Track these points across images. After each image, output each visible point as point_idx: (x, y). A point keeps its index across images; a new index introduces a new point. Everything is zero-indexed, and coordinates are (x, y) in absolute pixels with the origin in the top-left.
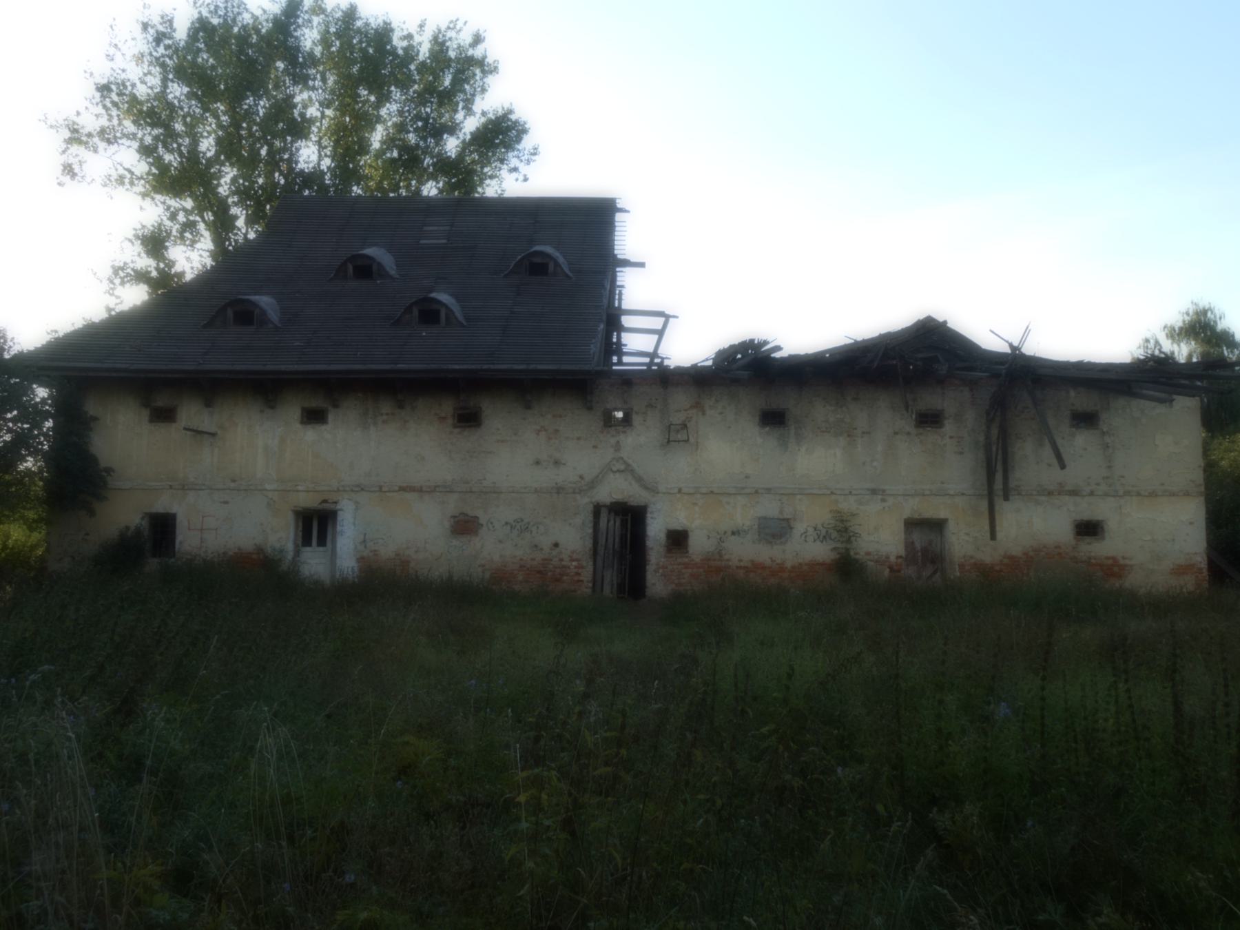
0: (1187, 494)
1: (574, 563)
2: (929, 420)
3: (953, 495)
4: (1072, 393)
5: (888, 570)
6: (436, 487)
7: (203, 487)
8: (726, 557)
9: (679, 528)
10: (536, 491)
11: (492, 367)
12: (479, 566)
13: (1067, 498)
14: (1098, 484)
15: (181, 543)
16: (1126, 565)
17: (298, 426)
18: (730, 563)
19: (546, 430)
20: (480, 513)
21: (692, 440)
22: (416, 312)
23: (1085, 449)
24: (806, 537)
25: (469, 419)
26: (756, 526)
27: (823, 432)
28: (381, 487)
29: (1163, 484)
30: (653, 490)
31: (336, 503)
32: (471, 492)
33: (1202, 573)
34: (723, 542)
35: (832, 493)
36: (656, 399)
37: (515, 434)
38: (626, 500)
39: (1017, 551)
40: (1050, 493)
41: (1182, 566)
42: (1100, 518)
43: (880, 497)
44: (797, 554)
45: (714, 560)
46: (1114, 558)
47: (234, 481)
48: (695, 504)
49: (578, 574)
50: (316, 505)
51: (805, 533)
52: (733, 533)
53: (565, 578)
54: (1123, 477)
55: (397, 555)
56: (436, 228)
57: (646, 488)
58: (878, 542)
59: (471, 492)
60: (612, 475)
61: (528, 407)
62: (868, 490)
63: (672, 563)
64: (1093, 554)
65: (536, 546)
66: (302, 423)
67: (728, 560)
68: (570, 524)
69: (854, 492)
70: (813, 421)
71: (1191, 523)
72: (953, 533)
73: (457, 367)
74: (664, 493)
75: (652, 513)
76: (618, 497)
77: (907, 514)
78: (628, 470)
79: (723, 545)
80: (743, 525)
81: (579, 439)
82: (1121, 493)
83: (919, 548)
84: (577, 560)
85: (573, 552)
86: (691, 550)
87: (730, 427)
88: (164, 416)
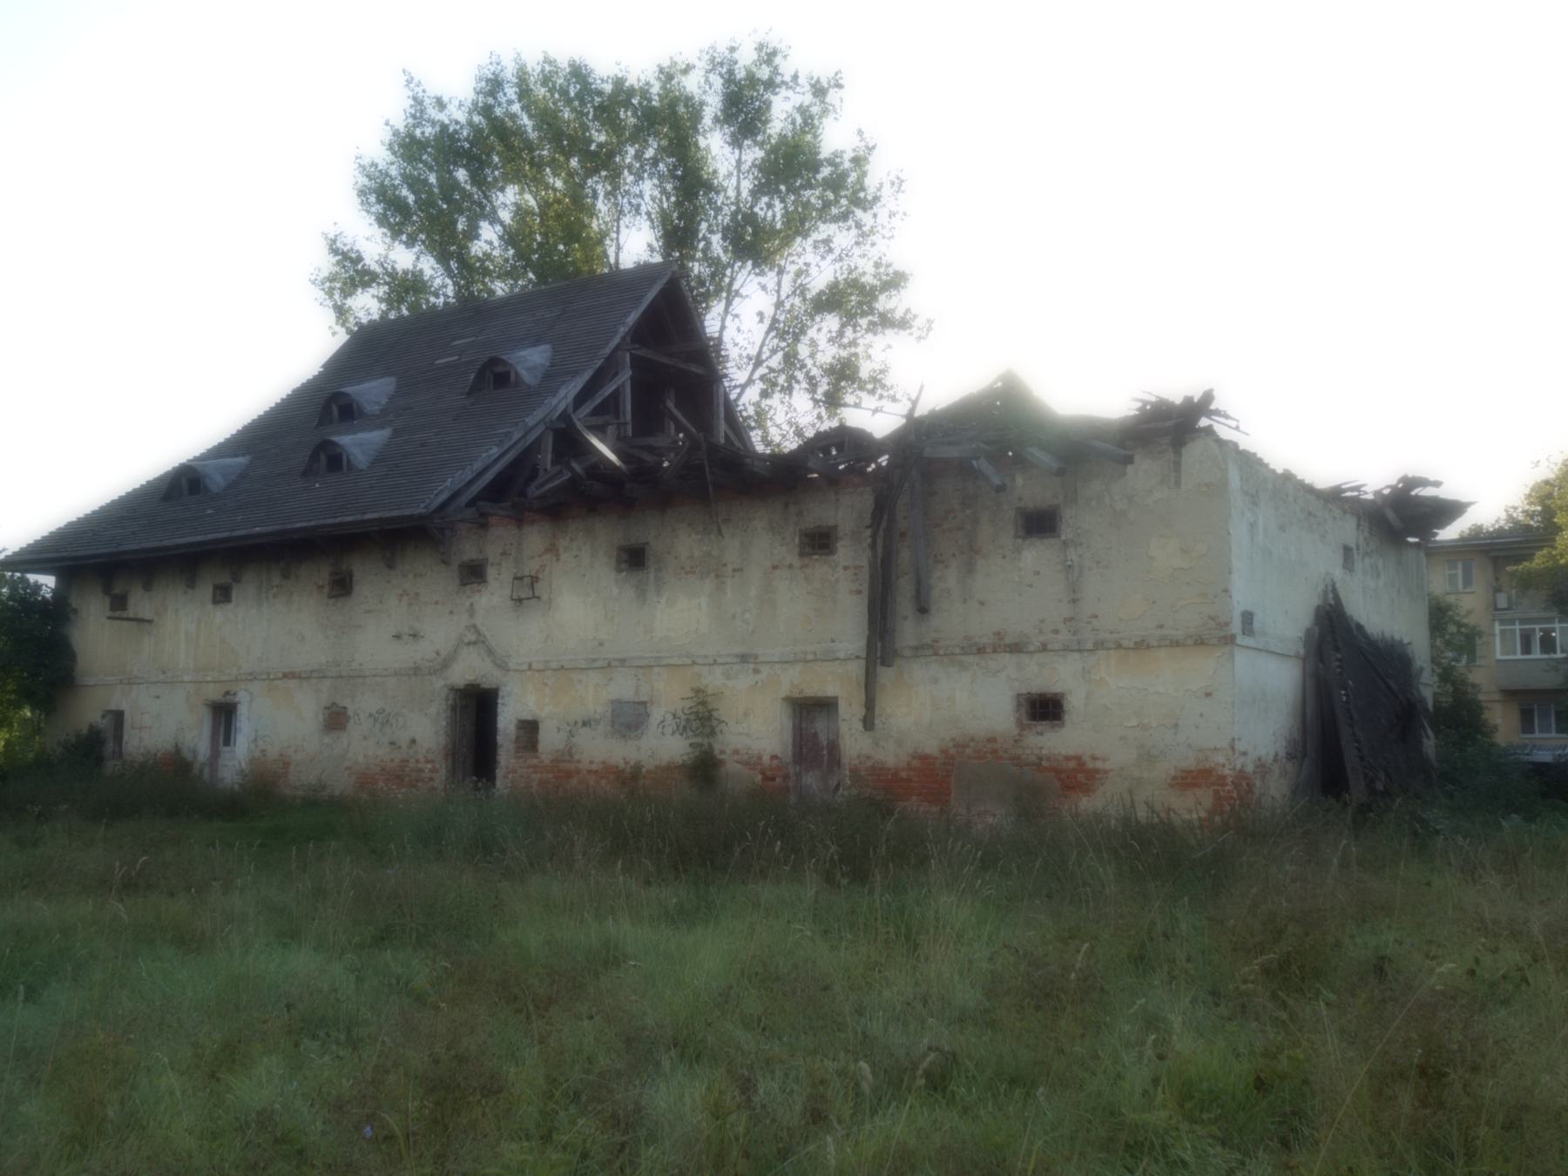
0: (1200, 642)
1: (429, 766)
2: (819, 542)
3: (843, 660)
6: (312, 672)
7: (142, 681)
8: (577, 757)
9: (530, 718)
10: (396, 674)
11: (330, 521)
12: (346, 769)
13: (1007, 655)
14: (1056, 632)
15: (126, 743)
16: (1097, 771)
17: (210, 606)
19: (408, 595)
20: (347, 703)
21: (545, 597)
22: (323, 458)
23: (1037, 573)
24: (663, 727)
25: (342, 587)
26: (609, 714)
27: (687, 573)
28: (268, 674)
29: (1161, 626)
30: (503, 666)
32: (341, 677)
33: (1226, 784)
34: (573, 736)
35: (694, 663)
36: (511, 544)
37: (381, 602)
38: (478, 682)
39: (931, 747)
40: (981, 651)
41: (1191, 772)
42: (1059, 690)
43: (752, 666)
44: (653, 753)
45: (564, 761)
46: (1078, 758)
47: (164, 673)
48: (546, 684)
49: (432, 779)
51: (662, 722)
52: (584, 724)
54: (1096, 617)
55: (281, 755)
56: (463, 341)
57: (498, 666)
58: (748, 735)
59: (341, 677)
61: (391, 567)
62: (737, 656)
64: (1044, 752)
65: (392, 743)
66: (215, 602)
67: (579, 761)
70: (676, 558)
71: (1208, 695)
72: (844, 720)
73: (298, 525)
74: (515, 671)
75: (503, 697)
77: (784, 691)
78: (479, 641)
79: (574, 740)
80: (595, 712)
81: (437, 603)
82: (1090, 645)
83: (825, 743)
84: (432, 761)
85: (428, 751)
87: (584, 575)
88: (119, 603)
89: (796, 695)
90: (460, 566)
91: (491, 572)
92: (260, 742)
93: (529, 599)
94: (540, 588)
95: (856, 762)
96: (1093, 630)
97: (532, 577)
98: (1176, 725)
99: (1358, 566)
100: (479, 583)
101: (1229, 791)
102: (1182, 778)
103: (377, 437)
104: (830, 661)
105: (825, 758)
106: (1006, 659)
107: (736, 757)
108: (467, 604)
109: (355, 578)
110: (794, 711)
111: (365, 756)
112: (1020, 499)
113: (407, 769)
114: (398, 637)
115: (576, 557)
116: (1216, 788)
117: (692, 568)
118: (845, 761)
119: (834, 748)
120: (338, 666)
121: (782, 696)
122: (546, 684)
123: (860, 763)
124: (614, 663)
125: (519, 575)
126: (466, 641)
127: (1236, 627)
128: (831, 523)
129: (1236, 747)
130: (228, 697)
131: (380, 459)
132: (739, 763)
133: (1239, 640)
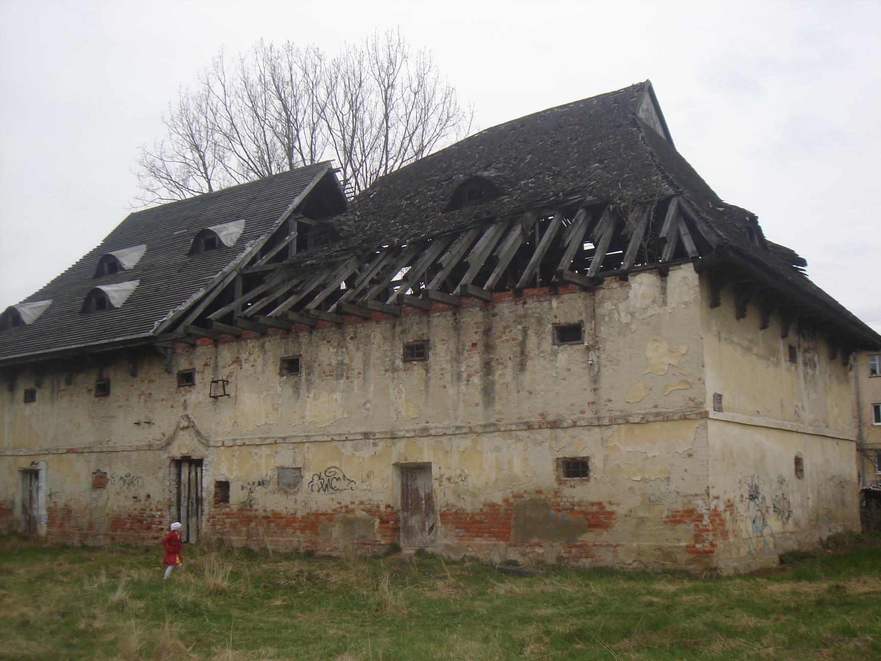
1: (159, 513)
4: (555, 303)
5: (378, 521)
9: (224, 480)
10: (138, 449)
14: (583, 412)
17: (22, 404)
18: (257, 513)
19: (144, 395)
20: (106, 470)
21: (233, 395)
22: (94, 301)
24: (312, 485)
25: (103, 390)
26: (276, 477)
27: (327, 376)
29: (656, 406)
31: (37, 464)
35: (333, 440)
37: (127, 400)
38: (189, 455)
39: (497, 498)
40: (529, 427)
43: (372, 441)
46: (600, 504)
48: (234, 456)
50: (28, 466)
52: (259, 484)
53: (153, 526)
54: (610, 401)
55: (66, 505)
60: (181, 432)
62: (361, 433)
64: (576, 500)
65: (135, 498)
67: (256, 510)
68: (156, 478)
69: (350, 437)
71: (690, 455)
73: (74, 347)
76: (184, 452)
79: (252, 495)
81: (163, 400)
83: (423, 496)
84: (160, 510)
85: (158, 502)
86: (231, 500)
89: (403, 462)
90: (177, 374)
91: (197, 378)
92: (53, 497)
93: (222, 396)
94: (229, 389)
95: (445, 509)
96: (609, 410)
97: (224, 381)
98: (668, 478)
99: (800, 359)
100: (190, 386)
101: (706, 526)
102: (674, 516)
103: (130, 286)
104: (425, 437)
105: (424, 507)
106: (547, 433)
107: (362, 507)
108: (182, 400)
109: (111, 384)
110: (402, 473)
111: (118, 506)
112: (556, 317)
113: (145, 515)
114: (138, 424)
115: (253, 366)
116: (697, 523)
117: (330, 372)
118: (437, 508)
119: (429, 498)
120: (101, 444)
121: (394, 460)
122: (234, 456)
123: (448, 510)
124: (278, 441)
125: (215, 379)
126: (181, 426)
127: (709, 406)
128: (425, 338)
129: (710, 493)
130: (34, 466)
131: (129, 301)
132: (364, 510)
133: (711, 416)
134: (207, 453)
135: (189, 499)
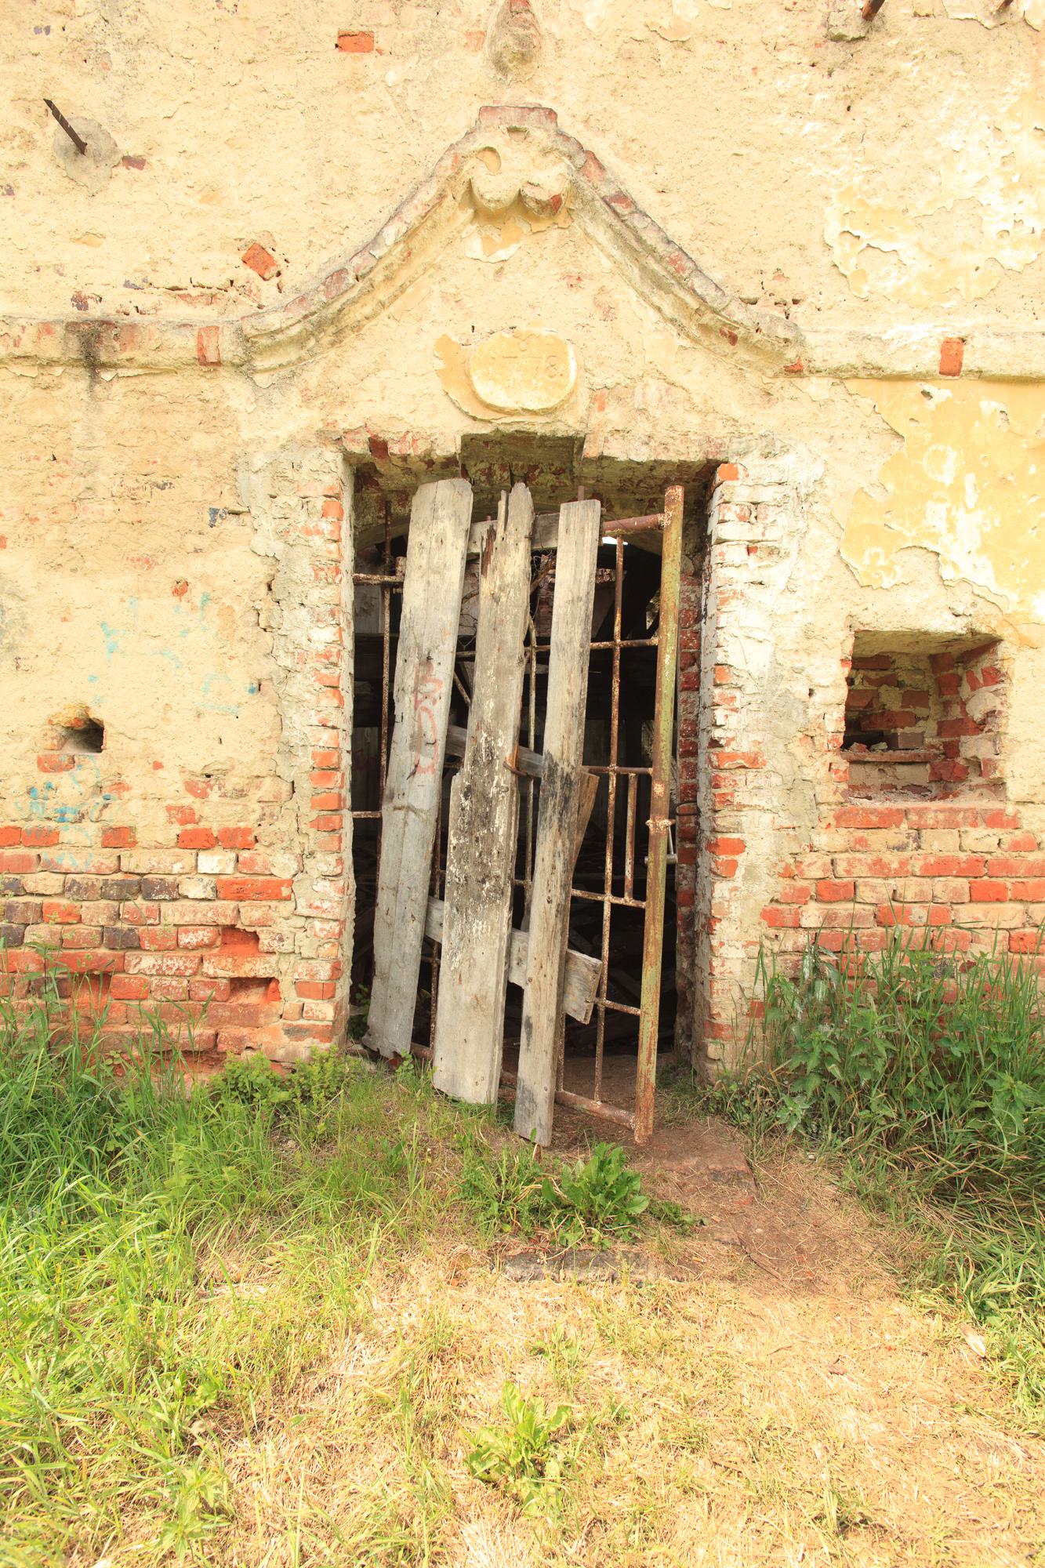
60: (473, 242)
63: (893, 860)
68: (181, 589)
74: (839, 375)
75: (753, 510)
84: (236, 840)
85: (204, 781)
134: (766, 420)
135: (451, 763)
